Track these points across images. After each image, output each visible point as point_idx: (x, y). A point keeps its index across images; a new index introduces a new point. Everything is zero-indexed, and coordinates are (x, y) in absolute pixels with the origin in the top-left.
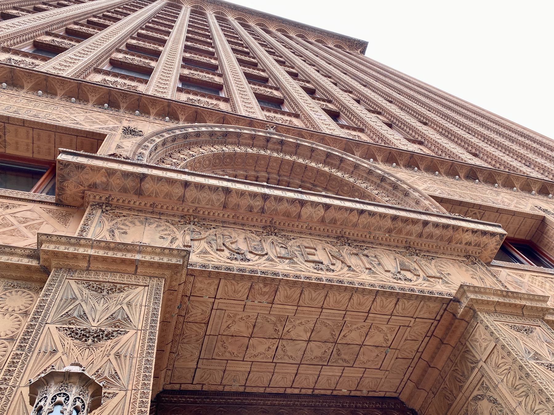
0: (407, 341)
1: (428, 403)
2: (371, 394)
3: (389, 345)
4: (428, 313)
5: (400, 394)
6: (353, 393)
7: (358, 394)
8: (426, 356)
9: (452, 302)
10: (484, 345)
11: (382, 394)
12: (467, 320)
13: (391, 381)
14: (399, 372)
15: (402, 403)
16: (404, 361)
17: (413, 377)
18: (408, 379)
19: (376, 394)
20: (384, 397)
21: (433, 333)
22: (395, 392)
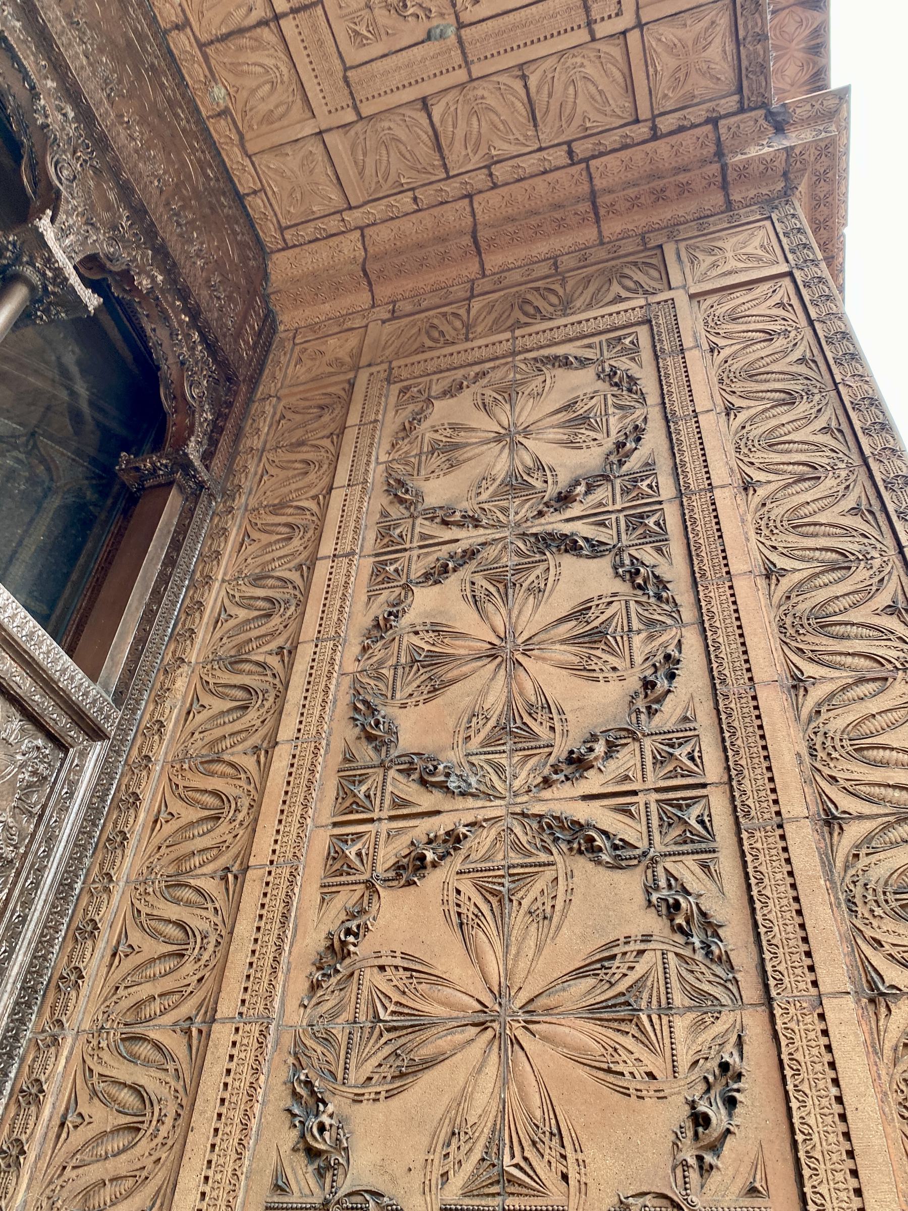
0: (518, 85)
1: (345, 327)
2: (220, 130)
3: (466, 17)
4: (672, 63)
5: (286, 248)
6: (181, 43)
7: (194, 72)
8: (490, 205)
9: (761, 112)
10: (733, 264)
11: (245, 183)
12: (736, 196)
13: (319, 169)
14: (369, 170)
15: (266, 276)
16: (425, 151)
17: (382, 235)
18: (361, 229)
19: (233, 157)
20: (239, 199)
21: (594, 157)
22: (282, 229)
